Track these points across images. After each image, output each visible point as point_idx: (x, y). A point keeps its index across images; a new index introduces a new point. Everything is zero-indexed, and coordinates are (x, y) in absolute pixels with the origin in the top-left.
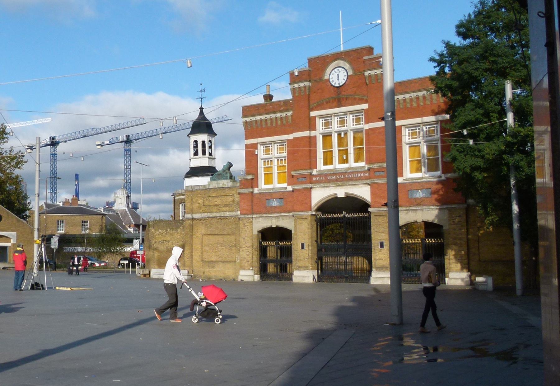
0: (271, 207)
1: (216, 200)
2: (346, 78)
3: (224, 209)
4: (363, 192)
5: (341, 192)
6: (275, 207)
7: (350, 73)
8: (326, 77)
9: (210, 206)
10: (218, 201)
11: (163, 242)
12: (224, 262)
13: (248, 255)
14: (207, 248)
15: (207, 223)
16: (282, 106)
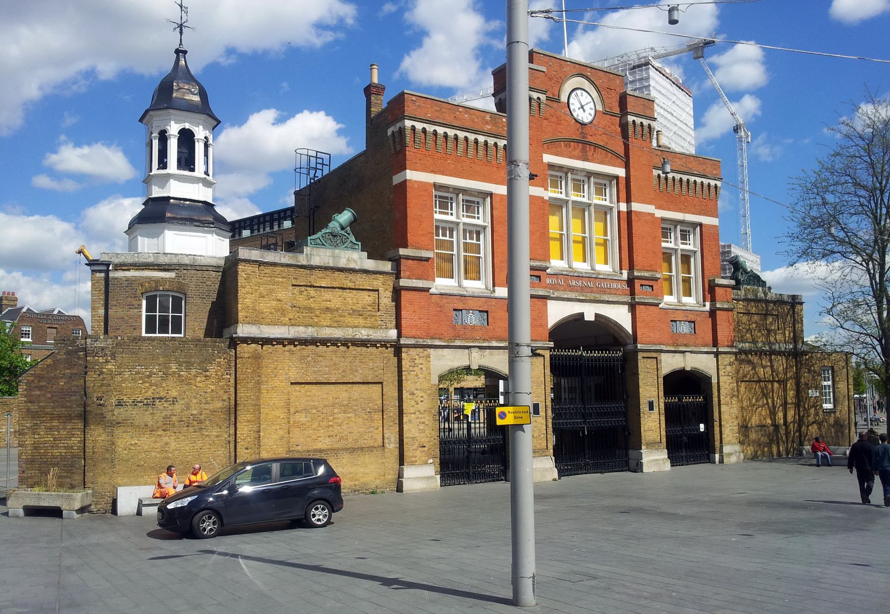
0: (465, 327)
1: (328, 295)
2: (593, 112)
3: (349, 320)
4: (620, 315)
5: (590, 312)
6: (473, 327)
7: (600, 108)
8: (564, 99)
9: (310, 309)
10: (334, 299)
11: (150, 403)
12: (352, 450)
13: (422, 431)
14: (302, 418)
15: (305, 353)
16: (487, 123)
